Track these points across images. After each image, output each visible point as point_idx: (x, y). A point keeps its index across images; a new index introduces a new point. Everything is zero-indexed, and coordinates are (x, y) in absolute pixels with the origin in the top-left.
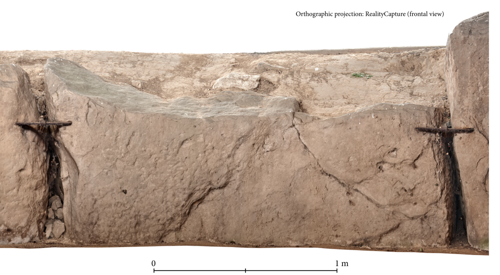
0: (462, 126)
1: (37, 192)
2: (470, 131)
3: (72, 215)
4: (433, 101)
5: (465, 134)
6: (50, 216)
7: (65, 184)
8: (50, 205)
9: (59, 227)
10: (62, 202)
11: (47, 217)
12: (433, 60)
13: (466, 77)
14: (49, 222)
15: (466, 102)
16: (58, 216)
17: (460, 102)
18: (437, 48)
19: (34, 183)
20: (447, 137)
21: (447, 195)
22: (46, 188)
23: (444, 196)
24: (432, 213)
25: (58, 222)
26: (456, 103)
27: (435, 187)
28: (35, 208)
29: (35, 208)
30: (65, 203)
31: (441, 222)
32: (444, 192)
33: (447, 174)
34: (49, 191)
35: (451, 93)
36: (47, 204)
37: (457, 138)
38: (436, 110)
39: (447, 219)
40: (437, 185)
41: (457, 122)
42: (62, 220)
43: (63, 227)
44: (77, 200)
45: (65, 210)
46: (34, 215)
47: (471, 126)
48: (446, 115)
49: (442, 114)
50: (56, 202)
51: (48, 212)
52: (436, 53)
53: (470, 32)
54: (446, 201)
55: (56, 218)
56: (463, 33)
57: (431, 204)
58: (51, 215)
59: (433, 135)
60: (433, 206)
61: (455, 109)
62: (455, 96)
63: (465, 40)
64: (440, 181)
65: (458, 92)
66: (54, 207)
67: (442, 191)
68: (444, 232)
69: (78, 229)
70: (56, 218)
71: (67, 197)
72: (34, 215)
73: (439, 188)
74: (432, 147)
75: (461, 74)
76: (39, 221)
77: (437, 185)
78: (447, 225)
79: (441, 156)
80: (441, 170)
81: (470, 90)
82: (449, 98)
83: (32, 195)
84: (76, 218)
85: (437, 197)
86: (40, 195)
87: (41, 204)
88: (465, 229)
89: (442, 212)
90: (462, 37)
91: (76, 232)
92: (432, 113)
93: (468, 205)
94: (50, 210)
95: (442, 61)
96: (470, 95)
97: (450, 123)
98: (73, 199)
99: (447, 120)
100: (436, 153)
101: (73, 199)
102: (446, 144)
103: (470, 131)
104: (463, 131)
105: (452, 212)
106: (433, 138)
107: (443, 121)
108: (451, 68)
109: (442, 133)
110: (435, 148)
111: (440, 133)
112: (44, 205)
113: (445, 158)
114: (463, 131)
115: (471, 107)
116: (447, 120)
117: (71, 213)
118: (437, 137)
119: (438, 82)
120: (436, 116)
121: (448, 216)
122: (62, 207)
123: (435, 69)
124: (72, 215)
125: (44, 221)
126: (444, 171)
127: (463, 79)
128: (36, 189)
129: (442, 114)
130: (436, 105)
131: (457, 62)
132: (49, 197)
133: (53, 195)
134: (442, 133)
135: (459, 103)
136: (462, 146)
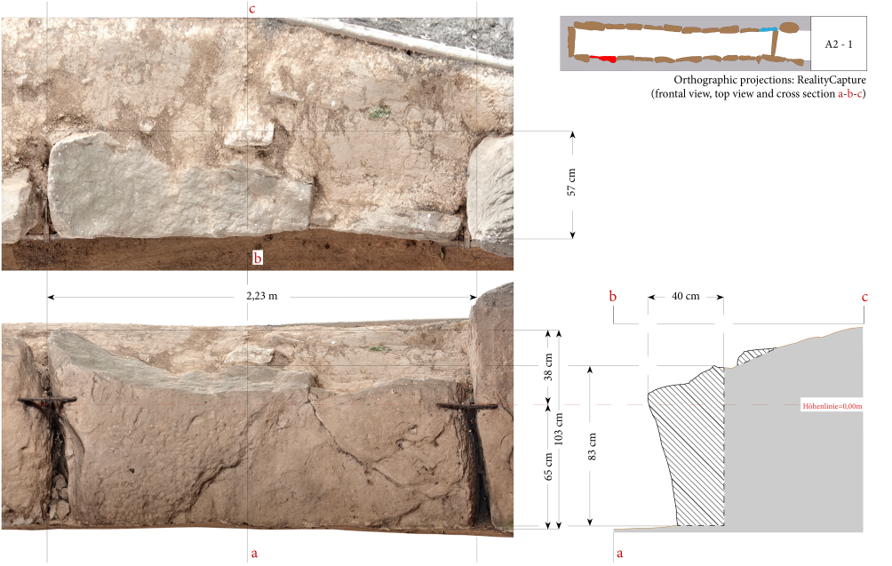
0: (486, 402)
2: (494, 407)
3: (77, 495)
4: (455, 376)
5: (489, 410)
6: (53, 496)
7: (70, 463)
8: (54, 485)
9: (63, 508)
10: (67, 482)
12: (455, 333)
13: (490, 351)
14: (53, 502)
15: (490, 376)
16: (63, 496)
17: (484, 377)
18: (460, 320)
20: (470, 413)
21: (470, 474)
23: (466, 475)
24: (454, 493)
25: (63, 502)
26: (479, 378)
27: (457, 465)
30: (70, 482)
31: (464, 502)
32: (467, 471)
33: (470, 452)
34: (53, 470)
35: (474, 368)
37: (480, 414)
38: (459, 385)
39: (470, 499)
40: (459, 464)
41: (481, 398)
42: (67, 500)
43: (68, 507)
44: (83, 479)
45: (70, 490)
47: (494, 402)
48: (468, 391)
49: (465, 390)
50: (60, 482)
52: (458, 325)
53: (494, 303)
54: (469, 480)
55: (60, 498)
56: (487, 305)
57: (453, 484)
58: (55, 495)
59: (456, 411)
60: (455, 485)
61: (478, 385)
62: (478, 370)
63: (488, 312)
64: (463, 459)
65: (481, 366)
66: (58, 486)
67: (464, 470)
68: (467, 513)
69: (83, 509)
70: (60, 498)
71: (71, 477)
73: (462, 467)
74: (454, 424)
75: (485, 348)
77: (459, 464)
78: (470, 505)
79: (463, 433)
80: (463, 448)
81: (494, 363)
82: (472, 373)
85: (459, 476)
88: (489, 510)
89: (464, 492)
90: (486, 309)
91: (81, 513)
92: (454, 389)
93: (491, 485)
94: (54, 490)
95: (464, 335)
96: (494, 369)
97: (473, 399)
98: (78, 478)
99: (470, 395)
100: (458, 430)
101: (78, 478)
102: (469, 421)
103: (494, 407)
104: (487, 407)
105: (475, 492)
106: (455, 415)
107: (466, 397)
108: (474, 341)
109: (465, 409)
110: (458, 425)
111: (462, 409)
113: (468, 436)
114: (487, 407)
115: (494, 382)
116: (470, 395)
118: (460, 414)
119: (460, 356)
120: (458, 391)
121: (470, 496)
122: (66, 487)
123: (457, 342)
124: (77, 495)
126: (466, 449)
127: (486, 353)
129: (465, 390)
130: (458, 380)
131: (480, 335)
132: (53, 477)
133: (57, 474)
134: (465, 409)
135: (482, 377)
136: (485, 422)
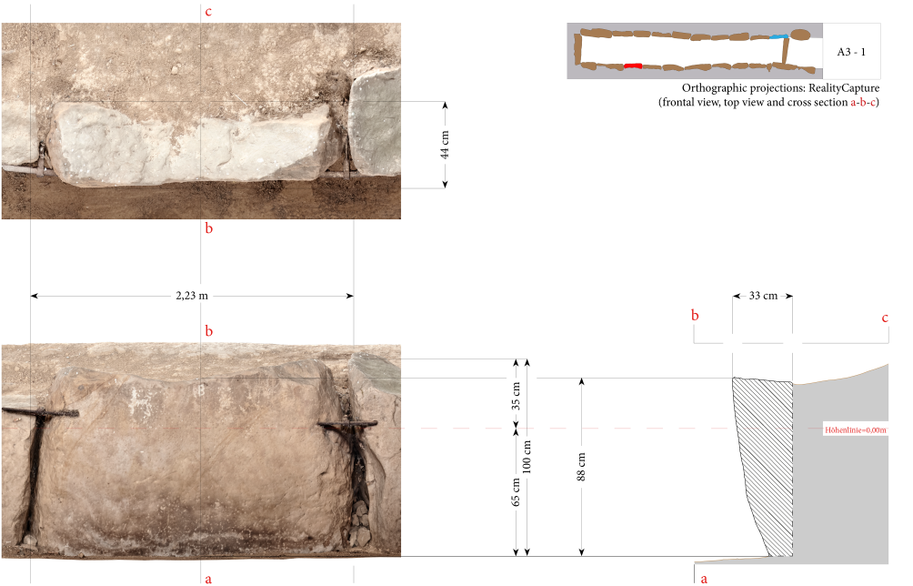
1: (341, 497)
3: (378, 522)
6: (354, 523)
7: (371, 489)
8: (354, 511)
10: (368, 508)
11: (351, 525)
14: (354, 529)
16: (364, 522)
19: (337, 487)
22: (350, 492)
25: (363, 529)
28: (338, 514)
29: (338, 514)
34: (354, 496)
36: (352, 509)
42: (368, 527)
45: (371, 517)
46: (337, 522)
50: (361, 508)
51: (352, 518)
55: (361, 525)
58: (356, 521)
66: (359, 513)
70: (361, 525)
71: (372, 503)
72: (337, 522)
76: (343, 529)
83: (334, 499)
84: (382, 526)
86: (344, 500)
87: (345, 510)
94: (355, 516)
98: (379, 504)
101: (379, 504)
112: (348, 511)
117: (376, 520)
122: (367, 513)
125: (347, 528)
128: (339, 494)
132: (354, 503)
133: (357, 500)
